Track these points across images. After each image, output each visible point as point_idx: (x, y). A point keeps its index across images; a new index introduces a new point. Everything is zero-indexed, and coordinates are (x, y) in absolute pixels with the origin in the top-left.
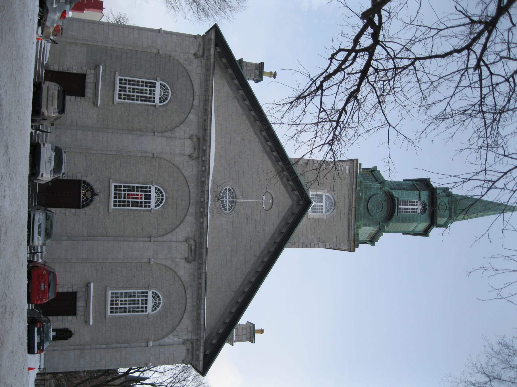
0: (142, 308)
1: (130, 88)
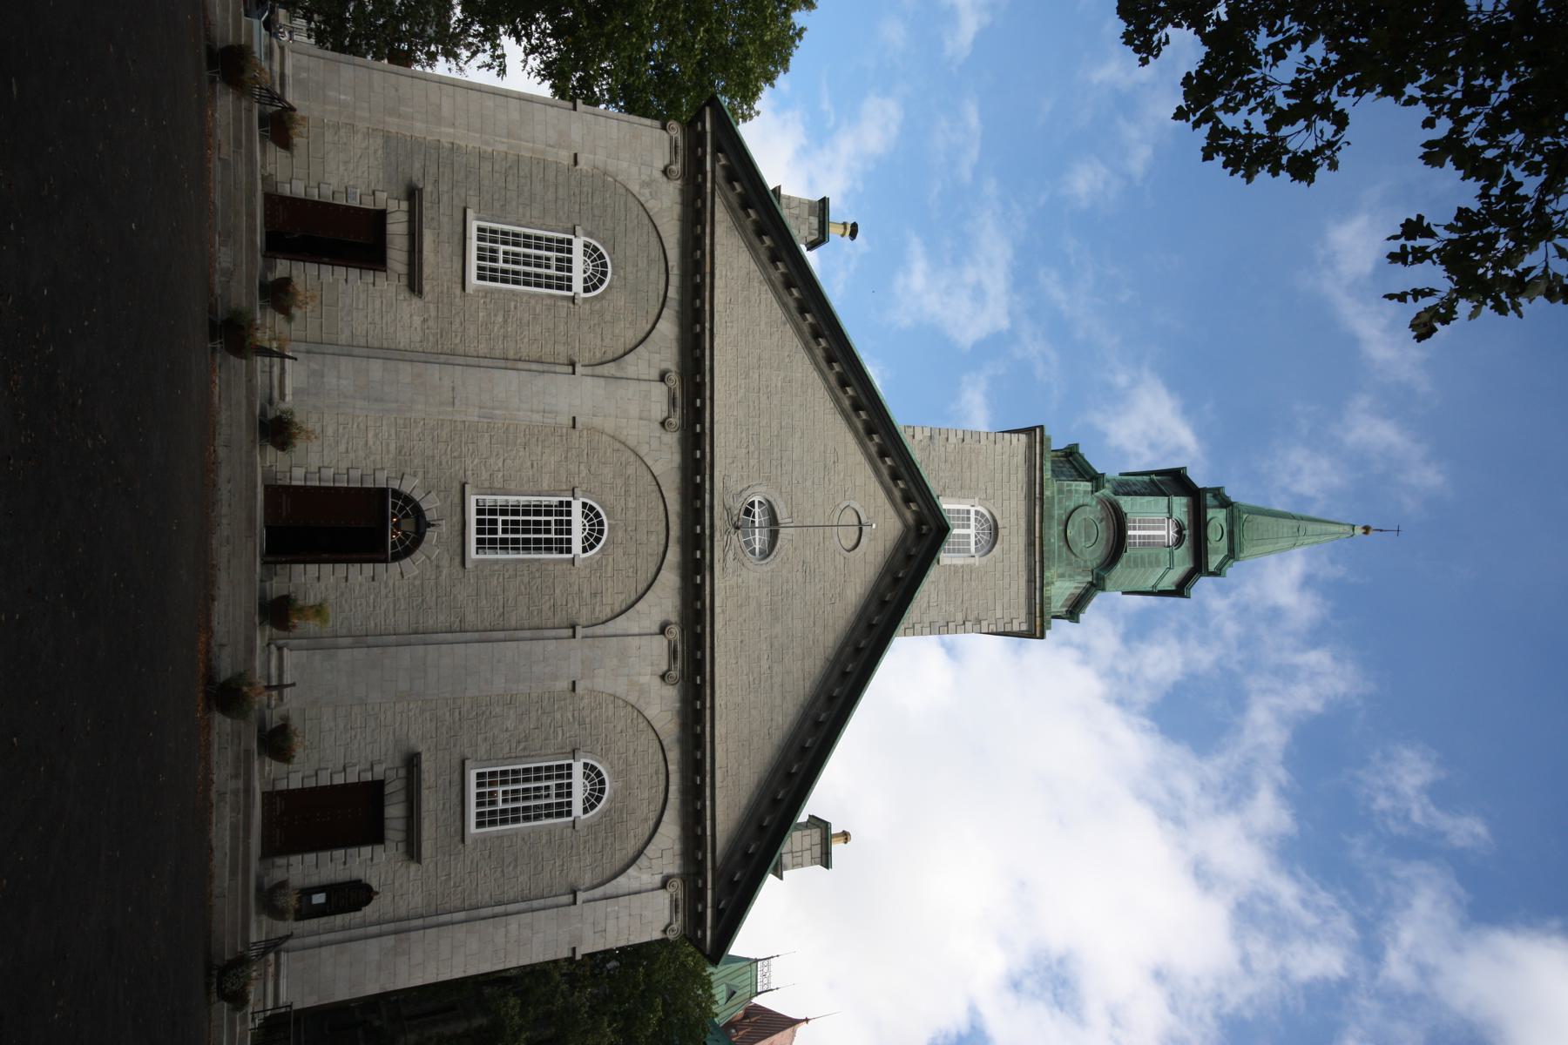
0: (559, 805)
1: (505, 253)
